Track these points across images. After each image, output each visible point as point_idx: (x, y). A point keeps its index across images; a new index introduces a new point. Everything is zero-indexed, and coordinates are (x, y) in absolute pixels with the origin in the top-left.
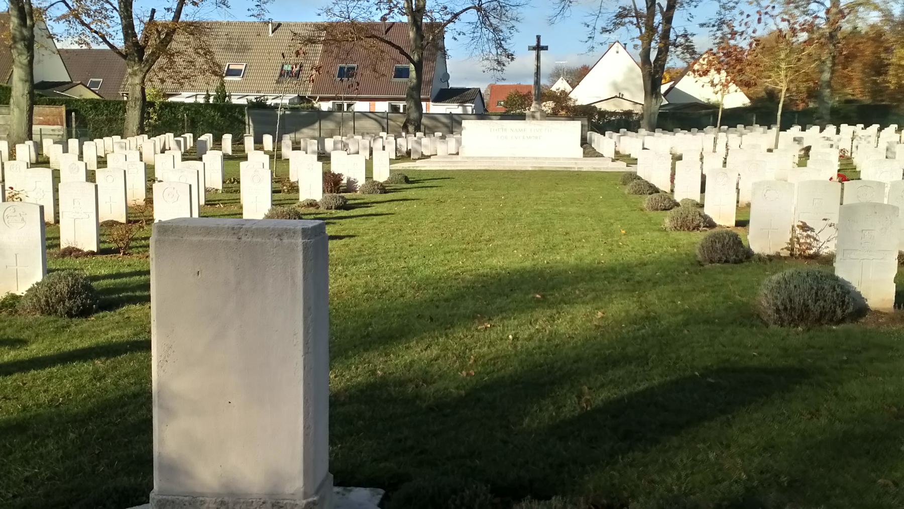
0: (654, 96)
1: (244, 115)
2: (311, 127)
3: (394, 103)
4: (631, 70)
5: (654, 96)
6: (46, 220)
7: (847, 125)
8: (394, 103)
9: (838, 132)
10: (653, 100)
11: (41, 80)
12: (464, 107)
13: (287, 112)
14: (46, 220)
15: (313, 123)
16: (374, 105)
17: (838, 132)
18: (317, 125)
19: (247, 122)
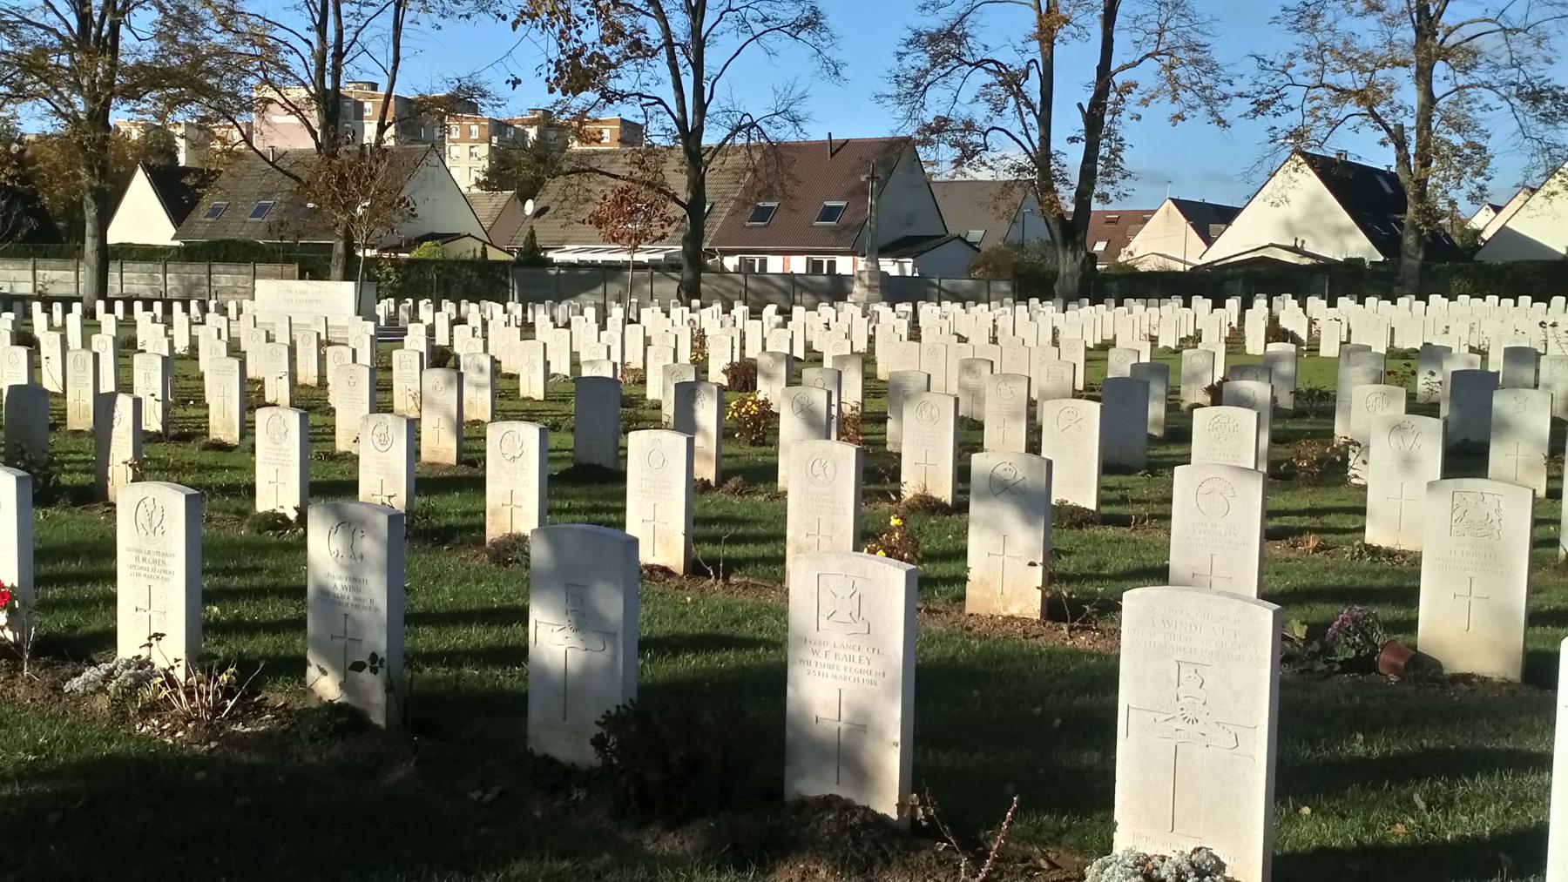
0: (1069, 247)
1: (507, 276)
2: (593, 291)
3: (816, 258)
4: (1317, 199)
5: (1069, 247)
6: (301, 379)
7: (1440, 296)
8: (816, 258)
9: (1516, 305)
10: (1069, 254)
11: (429, 232)
12: (901, 264)
13: (562, 272)
14: (301, 379)
15: (595, 286)
16: (789, 261)
17: (1516, 305)
18: (600, 289)
19: (511, 285)
